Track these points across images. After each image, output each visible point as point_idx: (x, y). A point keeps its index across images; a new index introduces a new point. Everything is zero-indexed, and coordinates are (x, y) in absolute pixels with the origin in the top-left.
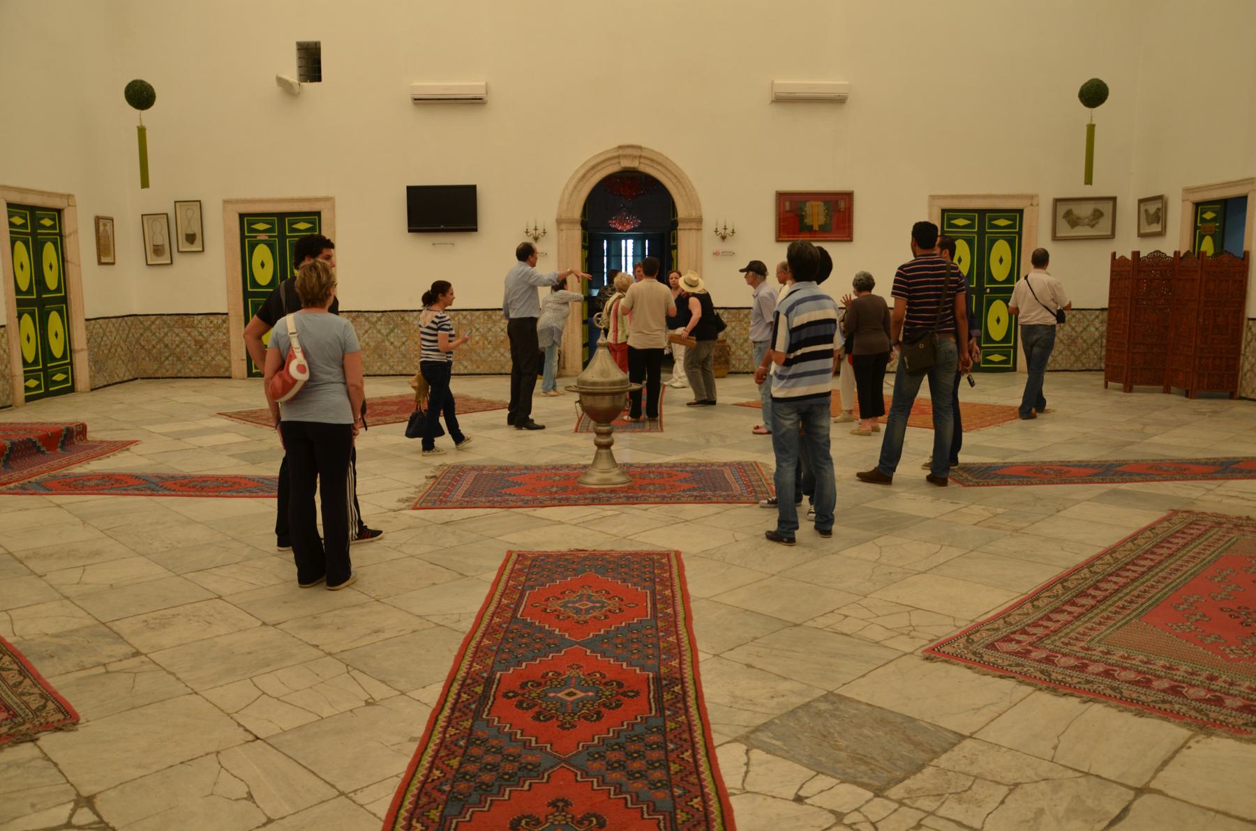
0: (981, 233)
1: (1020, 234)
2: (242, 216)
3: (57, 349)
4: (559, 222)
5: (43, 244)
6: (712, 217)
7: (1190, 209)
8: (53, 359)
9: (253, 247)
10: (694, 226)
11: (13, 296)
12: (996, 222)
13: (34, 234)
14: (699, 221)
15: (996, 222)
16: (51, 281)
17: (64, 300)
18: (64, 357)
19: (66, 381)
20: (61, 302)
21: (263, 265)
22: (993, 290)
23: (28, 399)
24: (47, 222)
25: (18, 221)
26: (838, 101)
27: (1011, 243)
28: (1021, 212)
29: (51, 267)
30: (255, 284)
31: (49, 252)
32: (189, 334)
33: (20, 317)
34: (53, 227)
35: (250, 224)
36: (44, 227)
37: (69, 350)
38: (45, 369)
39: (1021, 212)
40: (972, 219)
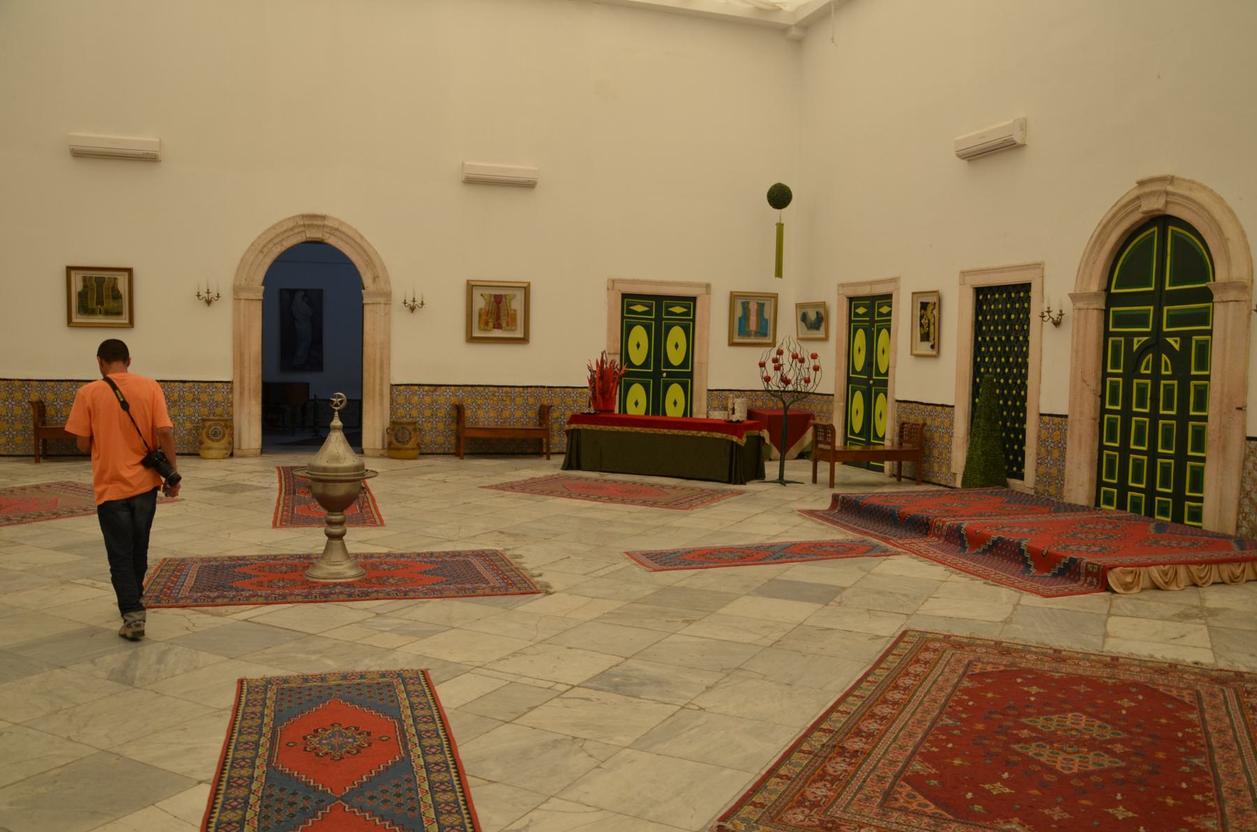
0: (658, 319)
1: (693, 320)
4: (237, 290)
6: (400, 292)
7: (845, 303)
10: (382, 300)
12: (672, 309)
14: (388, 295)
15: (672, 309)
22: (669, 375)
26: (529, 185)
27: (686, 329)
28: (694, 299)
39: (694, 299)
40: (650, 306)
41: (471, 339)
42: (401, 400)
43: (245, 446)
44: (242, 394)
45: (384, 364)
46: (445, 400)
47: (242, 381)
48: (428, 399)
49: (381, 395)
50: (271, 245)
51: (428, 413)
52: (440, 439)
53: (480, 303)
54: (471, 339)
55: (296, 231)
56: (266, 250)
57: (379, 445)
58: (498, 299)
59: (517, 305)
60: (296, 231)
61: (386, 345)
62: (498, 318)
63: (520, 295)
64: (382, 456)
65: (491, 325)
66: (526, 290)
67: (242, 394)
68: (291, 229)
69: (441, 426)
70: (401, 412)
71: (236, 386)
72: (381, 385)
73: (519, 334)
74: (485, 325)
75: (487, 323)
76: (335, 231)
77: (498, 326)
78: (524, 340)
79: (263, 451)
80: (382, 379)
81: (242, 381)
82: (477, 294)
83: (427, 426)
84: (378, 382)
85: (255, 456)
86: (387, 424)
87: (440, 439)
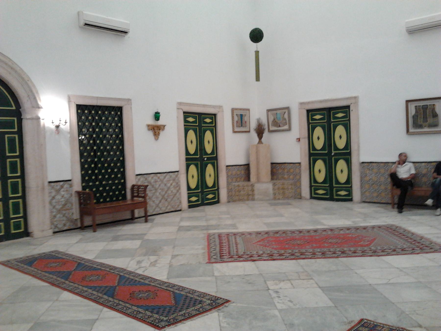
2: (308, 111)
3: (210, 181)
5: (205, 131)
8: (207, 187)
9: (314, 128)
11: (184, 157)
13: (200, 126)
16: (209, 148)
17: (216, 158)
18: (214, 186)
19: (214, 198)
20: (214, 159)
21: (318, 138)
23: (190, 207)
24: (208, 120)
25: (191, 119)
29: (209, 142)
30: (314, 149)
31: (208, 136)
32: (146, 179)
33: (188, 167)
34: (211, 123)
36: (206, 123)
37: (216, 183)
38: (202, 192)
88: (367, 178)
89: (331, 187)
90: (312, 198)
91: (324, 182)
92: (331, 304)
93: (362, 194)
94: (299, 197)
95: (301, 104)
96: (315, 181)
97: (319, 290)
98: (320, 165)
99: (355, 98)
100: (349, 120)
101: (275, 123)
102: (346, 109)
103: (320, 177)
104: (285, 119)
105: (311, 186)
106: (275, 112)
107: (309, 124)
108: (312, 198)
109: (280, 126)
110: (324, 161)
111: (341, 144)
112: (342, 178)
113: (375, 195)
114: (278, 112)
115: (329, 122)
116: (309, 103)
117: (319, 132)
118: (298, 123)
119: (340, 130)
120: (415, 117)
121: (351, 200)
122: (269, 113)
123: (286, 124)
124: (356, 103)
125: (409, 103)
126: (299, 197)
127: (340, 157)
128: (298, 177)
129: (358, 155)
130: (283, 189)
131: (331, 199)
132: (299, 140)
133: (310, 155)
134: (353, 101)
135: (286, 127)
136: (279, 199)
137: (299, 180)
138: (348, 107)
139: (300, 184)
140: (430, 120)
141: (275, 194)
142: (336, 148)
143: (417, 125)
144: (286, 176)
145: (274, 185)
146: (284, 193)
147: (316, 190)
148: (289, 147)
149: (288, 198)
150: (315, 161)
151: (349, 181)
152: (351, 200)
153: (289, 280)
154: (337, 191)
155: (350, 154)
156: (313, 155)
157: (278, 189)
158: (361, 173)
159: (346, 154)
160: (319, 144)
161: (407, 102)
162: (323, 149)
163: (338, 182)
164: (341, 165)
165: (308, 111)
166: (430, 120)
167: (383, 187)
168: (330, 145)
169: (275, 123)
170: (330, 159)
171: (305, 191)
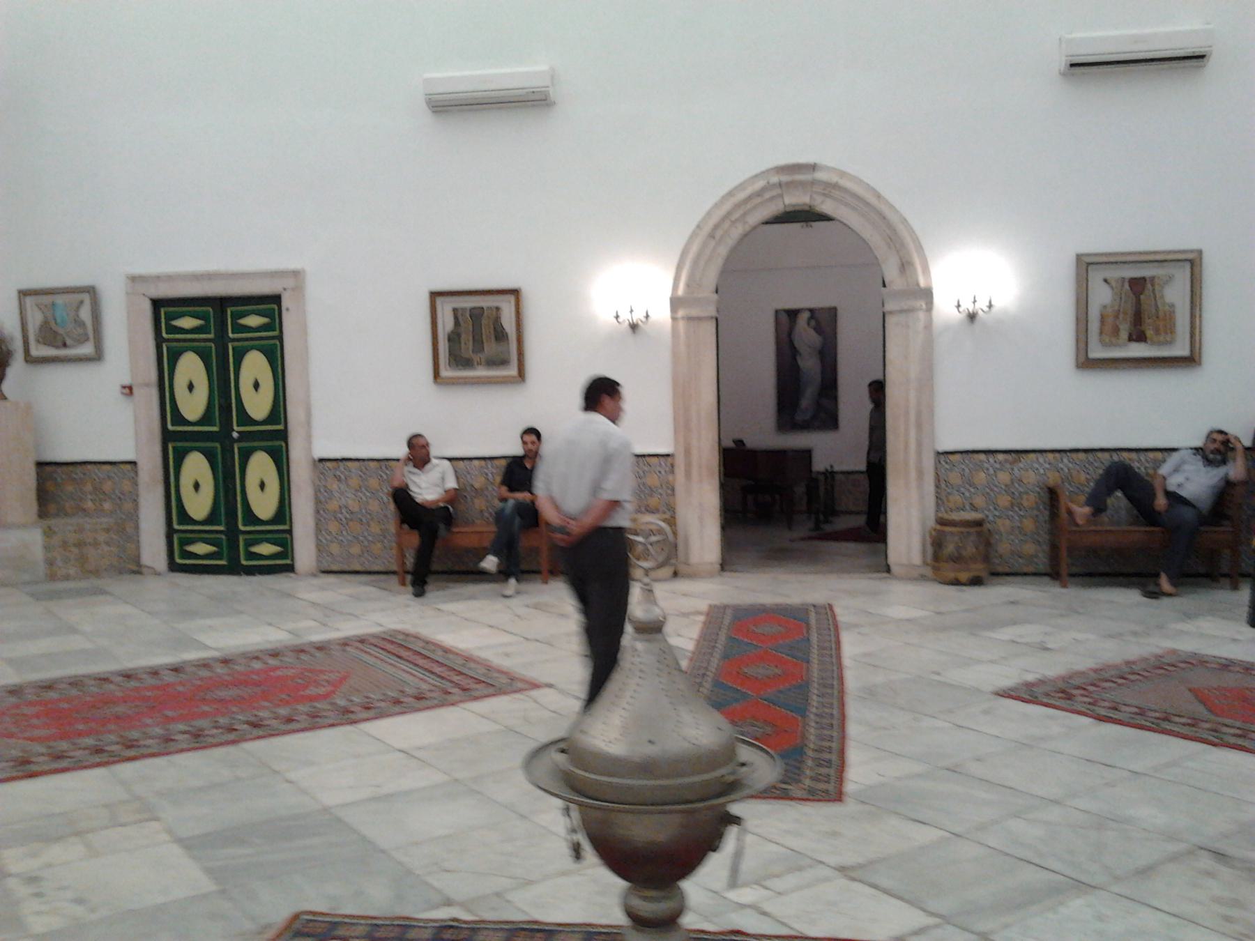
2: (157, 304)
9: (175, 357)
30: (179, 418)
35: (170, 317)
41: (1086, 363)
42: (955, 478)
43: (695, 558)
44: (688, 474)
45: (924, 419)
46: (1033, 475)
47: (688, 452)
48: (1004, 477)
49: (920, 473)
50: (727, 225)
51: (1004, 501)
52: (1029, 548)
53: (1102, 296)
54: (1086, 363)
55: (767, 195)
56: (719, 233)
57: (917, 559)
58: (1137, 285)
59: (1175, 294)
60: (767, 195)
61: (927, 382)
62: (1138, 318)
63: (1182, 277)
64: (923, 578)
65: (1124, 335)
66: (1193, 263)
67: (688, 474)
68: (759, 194)
69: (1029, 524)
70: (956, 498)
71: (680, 462)
72: (919, 453)
73: (1181, 350)
74: (1110, 332)
75: (1116, 331)
76: (830, 188)
77: (1138, 336)
78: (1191, 361)
79: (724, 566)
80: (919, 444)
81: (688, 452)
82: (1096, 277)
83: (1003, 525)
84: (913, 446)
85: (710, 575)
86: (931, 523)
87: (1029, 548)
88: (333, 505)
89: (232, 533)
90: (174, 567)
91: (212, 518)
92: (207, 885)
93: (320, 548)
94: (136, 568)
95: (134, 279)
96: (185, 517)
97: (176, 850)
98: (196, 467)
99: (296, 274)
100: (280, 338)
101: (50, 335)
102: (270, 304)
103: (199, 505)
104: (82, 324)
105: (170, 533)
106: (46, 300)
107: (159, 341)
108: (174, 567)
109: (65, 345)
110: (210, 456)
111: (258, 405)
112: (264, 505)
113: (355, 550)
114: (60, 300)
115: (221, 340)
116: (158, 278)
117: (191, 368)
118: (126, 340)
119: (254, 366)
120: (454, 338)
121: (290, 568)
122: (29, 301)
123: (83, 340)
124: (299, 289)
125: (439, 300)
126: (136, 568)
127: (256, 444)
128: (128, 506)
129: (309, 438)
130: (80, 545)
131: (234, 569)
132: (129, 390)
133: (167, 436)
134: (290, 283)
135: (87, 349)
136: (67, 578)
137: (134, 517)
138: (276, 299)
139: (137, 527)
140: (491, 348)
141: (50, 563)
142: (245, 418)
143: (459, 360)
144: (89, 505)
145: (49, 533)
146: (83, 559)
147: (184, 542)
148: (100, 411)
149: (96, 573)
150: (180, 457)
151: (283, 513)
152: (290, 568)
153: (78, 834)
154: (249, 544)
155: (283, 435)
156: (176, 439)
157: (65, 544)
158: (317, 491)
159: (274, 436)
160: (193, 405)
161: (434, 295)
162: (206, 419)
163: (251, 518)
164: (260, 466)
165: (157, 304)
166: (491, 348)
167: (375, 528)
168: (226, 409)
169: (50, 335)
170: (228, 451)
171: (153, 547)
